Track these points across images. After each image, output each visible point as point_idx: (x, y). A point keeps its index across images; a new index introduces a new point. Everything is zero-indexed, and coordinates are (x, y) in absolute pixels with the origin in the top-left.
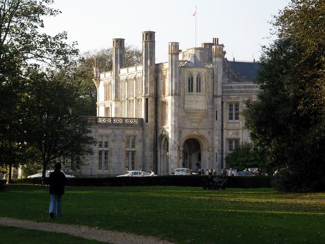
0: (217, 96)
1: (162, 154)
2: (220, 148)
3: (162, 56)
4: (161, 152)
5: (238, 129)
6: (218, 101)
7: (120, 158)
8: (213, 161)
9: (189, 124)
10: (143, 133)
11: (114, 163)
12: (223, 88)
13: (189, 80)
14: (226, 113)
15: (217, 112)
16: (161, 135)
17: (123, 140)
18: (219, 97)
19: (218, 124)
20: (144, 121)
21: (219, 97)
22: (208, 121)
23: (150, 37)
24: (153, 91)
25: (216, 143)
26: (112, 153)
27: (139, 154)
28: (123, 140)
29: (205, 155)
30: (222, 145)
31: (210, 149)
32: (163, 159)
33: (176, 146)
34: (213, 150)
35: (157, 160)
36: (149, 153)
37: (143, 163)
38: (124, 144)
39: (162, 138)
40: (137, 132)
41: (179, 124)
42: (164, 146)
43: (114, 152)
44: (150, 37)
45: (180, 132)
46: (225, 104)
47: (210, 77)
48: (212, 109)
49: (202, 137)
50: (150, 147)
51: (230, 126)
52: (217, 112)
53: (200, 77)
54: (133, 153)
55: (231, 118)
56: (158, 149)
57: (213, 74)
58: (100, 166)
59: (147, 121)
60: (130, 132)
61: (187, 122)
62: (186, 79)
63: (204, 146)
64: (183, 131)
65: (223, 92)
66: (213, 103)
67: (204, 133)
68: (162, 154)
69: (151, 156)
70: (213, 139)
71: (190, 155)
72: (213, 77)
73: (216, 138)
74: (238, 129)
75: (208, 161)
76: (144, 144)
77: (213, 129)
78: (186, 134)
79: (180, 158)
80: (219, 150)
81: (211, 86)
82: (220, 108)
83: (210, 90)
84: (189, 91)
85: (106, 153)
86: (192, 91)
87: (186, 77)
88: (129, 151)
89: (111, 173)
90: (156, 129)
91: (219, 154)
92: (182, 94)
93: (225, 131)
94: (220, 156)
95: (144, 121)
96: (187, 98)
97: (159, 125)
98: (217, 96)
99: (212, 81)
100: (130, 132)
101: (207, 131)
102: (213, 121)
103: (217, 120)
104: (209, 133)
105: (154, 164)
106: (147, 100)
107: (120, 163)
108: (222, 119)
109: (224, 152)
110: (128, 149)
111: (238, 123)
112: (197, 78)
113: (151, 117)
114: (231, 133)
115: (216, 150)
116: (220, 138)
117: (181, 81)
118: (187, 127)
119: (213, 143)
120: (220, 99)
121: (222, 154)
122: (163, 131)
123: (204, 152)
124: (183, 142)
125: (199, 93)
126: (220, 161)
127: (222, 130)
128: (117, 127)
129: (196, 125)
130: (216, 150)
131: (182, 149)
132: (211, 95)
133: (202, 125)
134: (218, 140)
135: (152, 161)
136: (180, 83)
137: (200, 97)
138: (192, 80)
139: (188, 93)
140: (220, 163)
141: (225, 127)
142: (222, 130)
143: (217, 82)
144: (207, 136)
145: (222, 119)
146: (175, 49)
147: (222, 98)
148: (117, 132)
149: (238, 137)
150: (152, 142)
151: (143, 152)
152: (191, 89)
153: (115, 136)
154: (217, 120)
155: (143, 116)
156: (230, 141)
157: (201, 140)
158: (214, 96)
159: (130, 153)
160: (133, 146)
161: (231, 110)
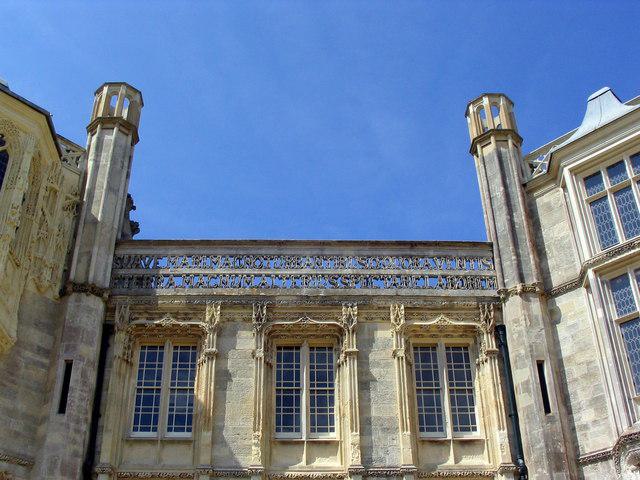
6: (88, 314)
14: (124, 387)
18: (96, 291)
21: (96, 291)
46: (120, 339)
55: (146, 420)
65: (117, 279)
66: (54, 321)
82: (91, 351)
83: (53, 256)
103: (62, 410)
108: (97, 414)
111: (187, 442)
120: (96, 304)
141: (105, 456)
145: (97, 414)
147: (109, 310)
154: (62, 410)
158: (70, 287)
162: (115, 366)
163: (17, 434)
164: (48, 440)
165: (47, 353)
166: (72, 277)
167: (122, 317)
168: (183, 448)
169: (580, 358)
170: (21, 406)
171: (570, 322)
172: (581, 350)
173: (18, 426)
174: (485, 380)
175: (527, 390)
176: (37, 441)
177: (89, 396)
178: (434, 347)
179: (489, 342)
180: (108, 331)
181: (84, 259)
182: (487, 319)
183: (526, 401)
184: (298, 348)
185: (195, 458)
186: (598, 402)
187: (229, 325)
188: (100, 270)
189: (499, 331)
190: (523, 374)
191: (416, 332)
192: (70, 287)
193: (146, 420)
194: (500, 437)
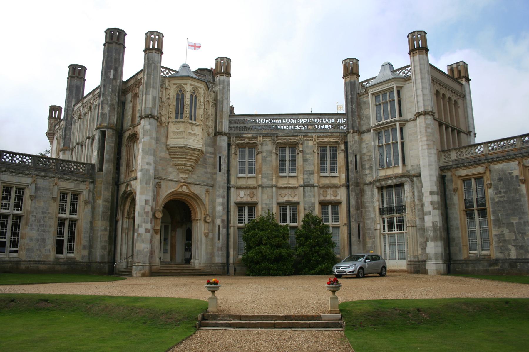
0: (222, 134)
1: (125, 226)
2: (225, 218)
3: (133, 63)
4: (122, 224)
5: (255, 188)
6: (223, 141)
7: (44, 231)
8: (213, 239)
9: (174, 174)
10: (94, 188)
11: (31, 239)
12: (230, 121)
13: (177, 99)
15: (220, 157)
16: (125, 192)
17: (54, 199)
19: (221, 178)
20: (97, 169)
22: (206, 173)
23: (115, 39)
24: (114, 119)
25: (219, 208)
26: (28, 219)
27: (83, 225)
28: (54, 199)
29: (200, 229)
30: (228, 212)
31: (209, 219)
32: (127, 234)
33: (148, 209)
34: (213, 222)
35: (116, 236)
36: (101, 225)
37: (90, 241)
38: (54, 207)
39: (127, 198)
40: (82, 187)
41: (156, 170)
42: (129, 213)
43: (32, 219)
44: (115, 39)
45: (158, 186)
46: (233, 147)
47: (211, 104)
48: (214, 153)
49: (196, 197)
50: (103, 212)
51: (242, 183)
52: (220, 157)
53: (196, 96)
54: (73, 223)
56: (119, 217)
57: (216, 99)
58: (59, 249)
59: (101, 169)
60: (68, 185)
61: (170, 170)
62: (171, 96)
63: (199, 214)
64: (163, 183)
65: (231, 128)
66: (214, 144)
67: (197, 190)
68: (125, 226)
69: (105, 230)
70: (213, 202)
71: (174, 230)
72: (215, 105)
73: (219, 200)
74: (255, 188)
75: (204, 238)
76: (93, 208)
77: (213, 186)
78: (167, 190)
79: (156, 232)
80: (223, 221)
81: (212, 118)
82: (225, 153)
83: (211, 123)
84: (177, 118)
85: (18, 218)
86: (182, 113)
87: (173, 91)
88: (65, 219)
89: (24, 258)
90: (117, 183)
91: (224, 227)
92: (164, 119)
93: (232, 190)
94: (225, 231)
95: (97, 169)
96: (173, 128)
97: (122, 177)
98: (222, 134)
99: (214, 111)
100: (68, 185)
101: (204, 189)
102: (215, 173)
103: (220, 171)
104: (207, 191)
105: (110, 244)
106: (103, 133)
107: (44, 240)
108: (229, 171)
109: (232, 223)
110: (63, 216)
111: (254, 177)
112: (192, 96)
113: (108, 161)
114: (242, 193)
115: (218, 222)
116: (225, 200)
117: (164, 99)
118: (172, 177)
119: (214, 208)
120: (225, 138)
121: (228, 227)
122: (128, 185)
123: (198, 224)
124: (161, 201)
125: (193, 122)
126: (225, 239)
127: (229, 189)
128: (43, 174)
129: (186, 176)
130: (218, 222)
131: (159, 215)
132: (212, 130)
133: (195, 177)
134: (223, 204)
135: (107, 238)
136: (162, 102)
137: (195, 128)
138: (183, 98)
139: (174, 120)
140: (225, 242)
141: (232, 183)
142: (229, 189)
143: (222, 111)
144: (203, 196)
145: (229, 171)
146: (154, 45)
147: (229, 138)
148: (42, 183)
149: (255, 199)
150: (109, 205)
151: (92, 223)
152: (179, 112)
153: (37, 189)
154: (220, 171)
155: (94, 160)
156: (241, 206)
157: (194, 203)
158: (217, 134)
159: (67, 223)
160: (73, 211)
161: (242, 157)
162: (232, 156)
163: (209, 178)
164: (217, 180)
165: (212, 153)
166: (218, 130)
167: (233, 141)
168: (253, 179)
169: (368, 154)
170: (209, 170)
171: (367, 143)
172: (368, 152)
173: (208, 176)
174: (341, 158)
175: (351, 163)
176: (215, 180)
177: (226, 166)
178: (326, 147)
179: (343, 147)
180: (229, 145)
181: (220, 124)
182: (342, 140)
183: (351, 166)
184: (285, 148)
185: (257, 182)
186: (371, 168)
187: (265, 142)
188: (225, 127)
189: (346, 144)
190: (351, 158)
191: (319, 143)
192: (217, 134)
193: (242, 171)
194: (343, 176)
